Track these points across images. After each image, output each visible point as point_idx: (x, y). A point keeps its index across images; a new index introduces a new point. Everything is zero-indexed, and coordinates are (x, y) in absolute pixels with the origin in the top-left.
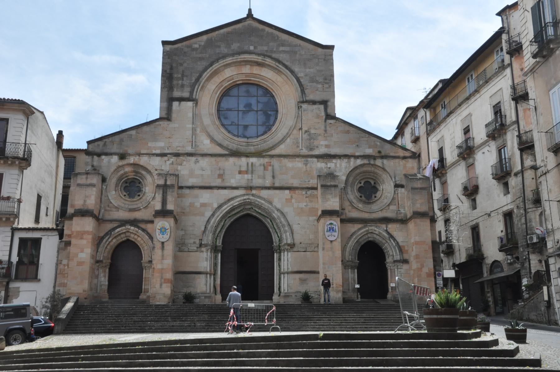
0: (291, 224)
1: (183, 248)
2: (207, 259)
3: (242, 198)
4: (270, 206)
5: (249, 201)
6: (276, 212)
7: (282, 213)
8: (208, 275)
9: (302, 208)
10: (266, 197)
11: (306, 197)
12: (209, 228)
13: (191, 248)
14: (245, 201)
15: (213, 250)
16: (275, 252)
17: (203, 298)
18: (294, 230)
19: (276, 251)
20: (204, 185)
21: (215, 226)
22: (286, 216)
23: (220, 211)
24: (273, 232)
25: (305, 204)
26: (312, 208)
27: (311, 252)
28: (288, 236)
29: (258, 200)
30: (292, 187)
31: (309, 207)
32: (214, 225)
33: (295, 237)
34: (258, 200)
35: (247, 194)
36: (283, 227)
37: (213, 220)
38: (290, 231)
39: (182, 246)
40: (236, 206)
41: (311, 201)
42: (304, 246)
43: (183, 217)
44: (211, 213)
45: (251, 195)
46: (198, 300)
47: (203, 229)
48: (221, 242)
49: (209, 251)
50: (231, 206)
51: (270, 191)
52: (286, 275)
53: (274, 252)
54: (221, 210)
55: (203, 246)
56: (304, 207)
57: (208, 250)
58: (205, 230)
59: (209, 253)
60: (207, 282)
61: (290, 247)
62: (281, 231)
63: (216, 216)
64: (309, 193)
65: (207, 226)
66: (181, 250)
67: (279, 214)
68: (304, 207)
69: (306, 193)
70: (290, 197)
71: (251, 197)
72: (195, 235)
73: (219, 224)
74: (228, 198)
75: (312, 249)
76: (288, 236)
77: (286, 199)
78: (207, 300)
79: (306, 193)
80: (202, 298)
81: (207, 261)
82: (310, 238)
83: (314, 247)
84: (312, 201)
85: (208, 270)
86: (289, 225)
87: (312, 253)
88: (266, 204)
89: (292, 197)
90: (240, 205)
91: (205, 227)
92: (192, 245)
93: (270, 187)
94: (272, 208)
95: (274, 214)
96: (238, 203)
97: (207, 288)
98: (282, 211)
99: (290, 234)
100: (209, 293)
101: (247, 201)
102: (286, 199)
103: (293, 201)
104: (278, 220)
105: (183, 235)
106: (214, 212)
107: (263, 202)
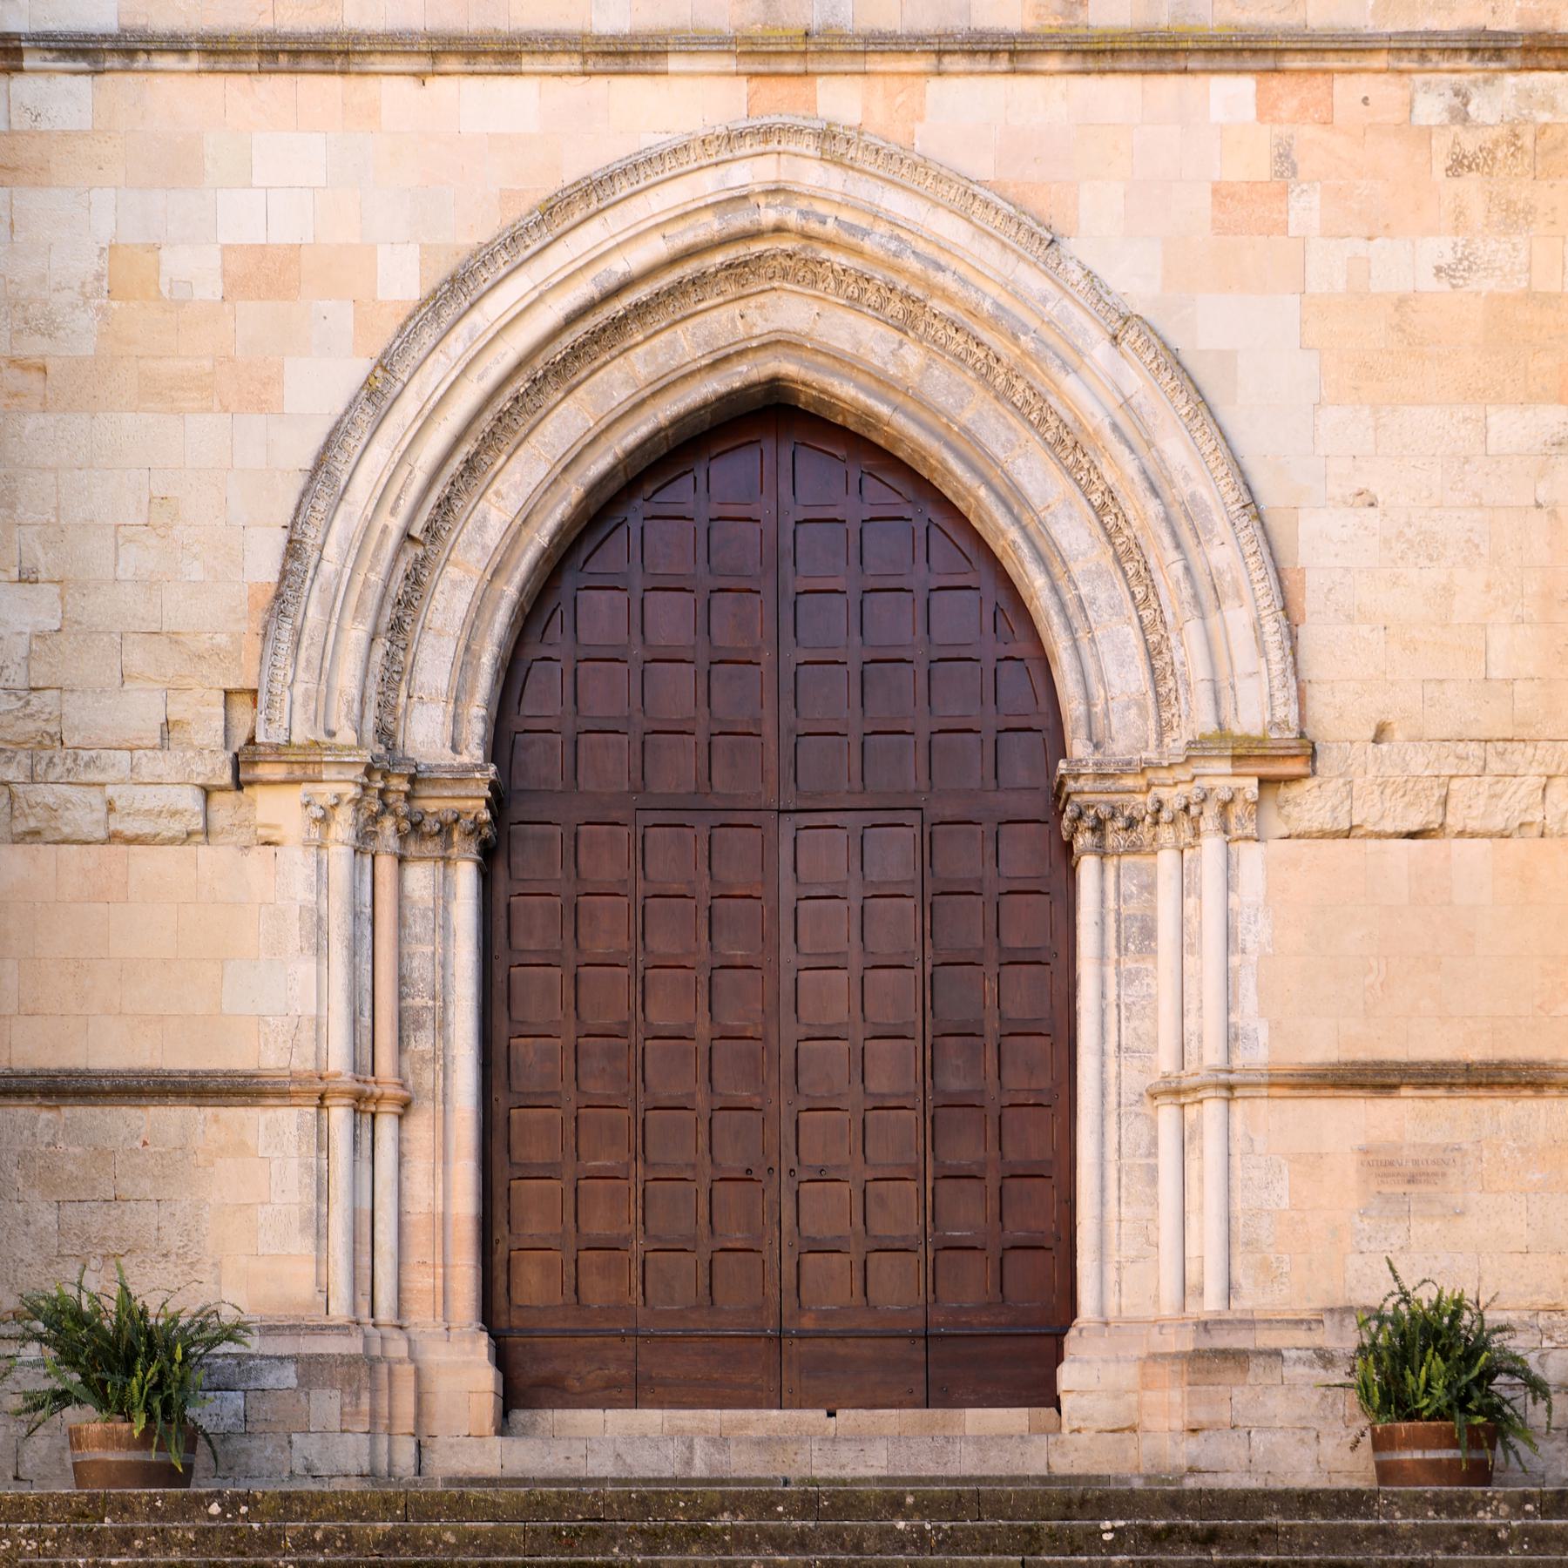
0: (1270, 496)
1: (46, 794)
2: (320, 924)
3: (708, 185)
4: (1033, 281)
5: (793, 219)
6: (1100, 351)
7: (1174, 363)
8: (339, 1116)
9: (1401, 302)
10: (982, 167)
11: (1459, 165)
12: (331, 551)
13: (151, 798)
14: (740, 220)
15: (388, 823)
16: (1083, 840)
17: (288, 1376)
18: (1313, 580)
19: (1099, 827)
20: (265, 23)
21: (408, 537)
22: (1213, 396)
23: (458, 345)
24: (1063, 607)
25: (1439, 248)
26: (1530, 296)
27: (1504, 835)
28: (1243, 654)
29: (895, 203)
30: (1288, 34)
31: (1486, 284)
32: (396, 525)
33: (1317, 665)
34: (895, 203)
35: (766, 133)
36: (1178, 546)
37: (379, 456)
38: (1265, 590)
39: (33, 779)
40: (642, 293)
41: (1514, 216)
42: (1419, 760)
43: (31, 423)
44: (357, 369)
45: (808, 146)
46: (236, 1400)
47: (265, 565)
48: (476, 729)
49: (343, 827)
50: (583, 291)
51: (1023, 88)
52: (1213, 1109)
53: (1068, 847)
54: (462, 329)
55: (264, 771)
56: (1428, 282)
57: (324, 820)
58: (284, 574)
59: (339, 858)
60: (323, 1191)
61: (1264, 782)
62: (1152, 586)
63: (407, 409)
64: (1492, 119)
65: (312, 535)
66: (20, 826)
67: (1136, 380)
68: (1428, 282)
69: (1460, 115)
70: (1263, 170)
71: (812, 174)
72: (174, 638)
73: (445, 506)
74: (548, 187)
75: (1518, 799)
76: (1243, 654)
77: (1222, 194)
78: (327, 1404)
79: (1460, 115)
80: (269, 1381)
81: (320, 950)
82: (1495, 673)
83: (1533, 782)
84: (1530, 210)
85: (338, 1060)
86: (1252, 507)
87: (1511, 844)
88: (990, 255)
89: (1285, 161)
90: (688, 269)
91: (293, 549)
92: (154, 764)
93: (1027, 36)
94: (1051, 309)
95: (1069, 383)
96: (655, 249)
97: (322, 1260)
98: (1175, 341)
99: (1258, 626)
100: (342, 1330)
101: (769, 217)
102: (1222, 194)
103: (1305, 209)
104: (1120, 450)
105: (40, 636)
106: (385, 364)
107: (948, 227)
